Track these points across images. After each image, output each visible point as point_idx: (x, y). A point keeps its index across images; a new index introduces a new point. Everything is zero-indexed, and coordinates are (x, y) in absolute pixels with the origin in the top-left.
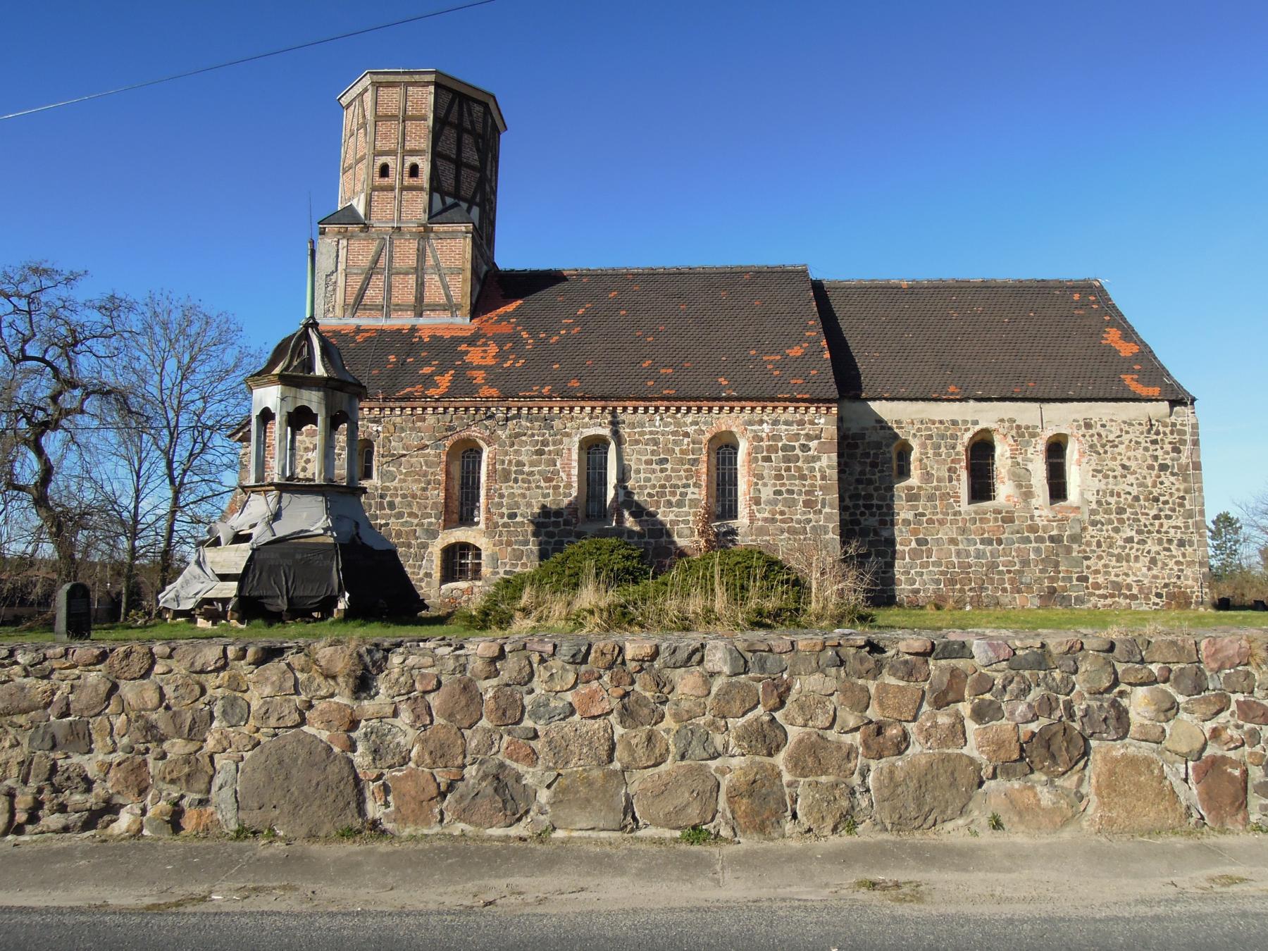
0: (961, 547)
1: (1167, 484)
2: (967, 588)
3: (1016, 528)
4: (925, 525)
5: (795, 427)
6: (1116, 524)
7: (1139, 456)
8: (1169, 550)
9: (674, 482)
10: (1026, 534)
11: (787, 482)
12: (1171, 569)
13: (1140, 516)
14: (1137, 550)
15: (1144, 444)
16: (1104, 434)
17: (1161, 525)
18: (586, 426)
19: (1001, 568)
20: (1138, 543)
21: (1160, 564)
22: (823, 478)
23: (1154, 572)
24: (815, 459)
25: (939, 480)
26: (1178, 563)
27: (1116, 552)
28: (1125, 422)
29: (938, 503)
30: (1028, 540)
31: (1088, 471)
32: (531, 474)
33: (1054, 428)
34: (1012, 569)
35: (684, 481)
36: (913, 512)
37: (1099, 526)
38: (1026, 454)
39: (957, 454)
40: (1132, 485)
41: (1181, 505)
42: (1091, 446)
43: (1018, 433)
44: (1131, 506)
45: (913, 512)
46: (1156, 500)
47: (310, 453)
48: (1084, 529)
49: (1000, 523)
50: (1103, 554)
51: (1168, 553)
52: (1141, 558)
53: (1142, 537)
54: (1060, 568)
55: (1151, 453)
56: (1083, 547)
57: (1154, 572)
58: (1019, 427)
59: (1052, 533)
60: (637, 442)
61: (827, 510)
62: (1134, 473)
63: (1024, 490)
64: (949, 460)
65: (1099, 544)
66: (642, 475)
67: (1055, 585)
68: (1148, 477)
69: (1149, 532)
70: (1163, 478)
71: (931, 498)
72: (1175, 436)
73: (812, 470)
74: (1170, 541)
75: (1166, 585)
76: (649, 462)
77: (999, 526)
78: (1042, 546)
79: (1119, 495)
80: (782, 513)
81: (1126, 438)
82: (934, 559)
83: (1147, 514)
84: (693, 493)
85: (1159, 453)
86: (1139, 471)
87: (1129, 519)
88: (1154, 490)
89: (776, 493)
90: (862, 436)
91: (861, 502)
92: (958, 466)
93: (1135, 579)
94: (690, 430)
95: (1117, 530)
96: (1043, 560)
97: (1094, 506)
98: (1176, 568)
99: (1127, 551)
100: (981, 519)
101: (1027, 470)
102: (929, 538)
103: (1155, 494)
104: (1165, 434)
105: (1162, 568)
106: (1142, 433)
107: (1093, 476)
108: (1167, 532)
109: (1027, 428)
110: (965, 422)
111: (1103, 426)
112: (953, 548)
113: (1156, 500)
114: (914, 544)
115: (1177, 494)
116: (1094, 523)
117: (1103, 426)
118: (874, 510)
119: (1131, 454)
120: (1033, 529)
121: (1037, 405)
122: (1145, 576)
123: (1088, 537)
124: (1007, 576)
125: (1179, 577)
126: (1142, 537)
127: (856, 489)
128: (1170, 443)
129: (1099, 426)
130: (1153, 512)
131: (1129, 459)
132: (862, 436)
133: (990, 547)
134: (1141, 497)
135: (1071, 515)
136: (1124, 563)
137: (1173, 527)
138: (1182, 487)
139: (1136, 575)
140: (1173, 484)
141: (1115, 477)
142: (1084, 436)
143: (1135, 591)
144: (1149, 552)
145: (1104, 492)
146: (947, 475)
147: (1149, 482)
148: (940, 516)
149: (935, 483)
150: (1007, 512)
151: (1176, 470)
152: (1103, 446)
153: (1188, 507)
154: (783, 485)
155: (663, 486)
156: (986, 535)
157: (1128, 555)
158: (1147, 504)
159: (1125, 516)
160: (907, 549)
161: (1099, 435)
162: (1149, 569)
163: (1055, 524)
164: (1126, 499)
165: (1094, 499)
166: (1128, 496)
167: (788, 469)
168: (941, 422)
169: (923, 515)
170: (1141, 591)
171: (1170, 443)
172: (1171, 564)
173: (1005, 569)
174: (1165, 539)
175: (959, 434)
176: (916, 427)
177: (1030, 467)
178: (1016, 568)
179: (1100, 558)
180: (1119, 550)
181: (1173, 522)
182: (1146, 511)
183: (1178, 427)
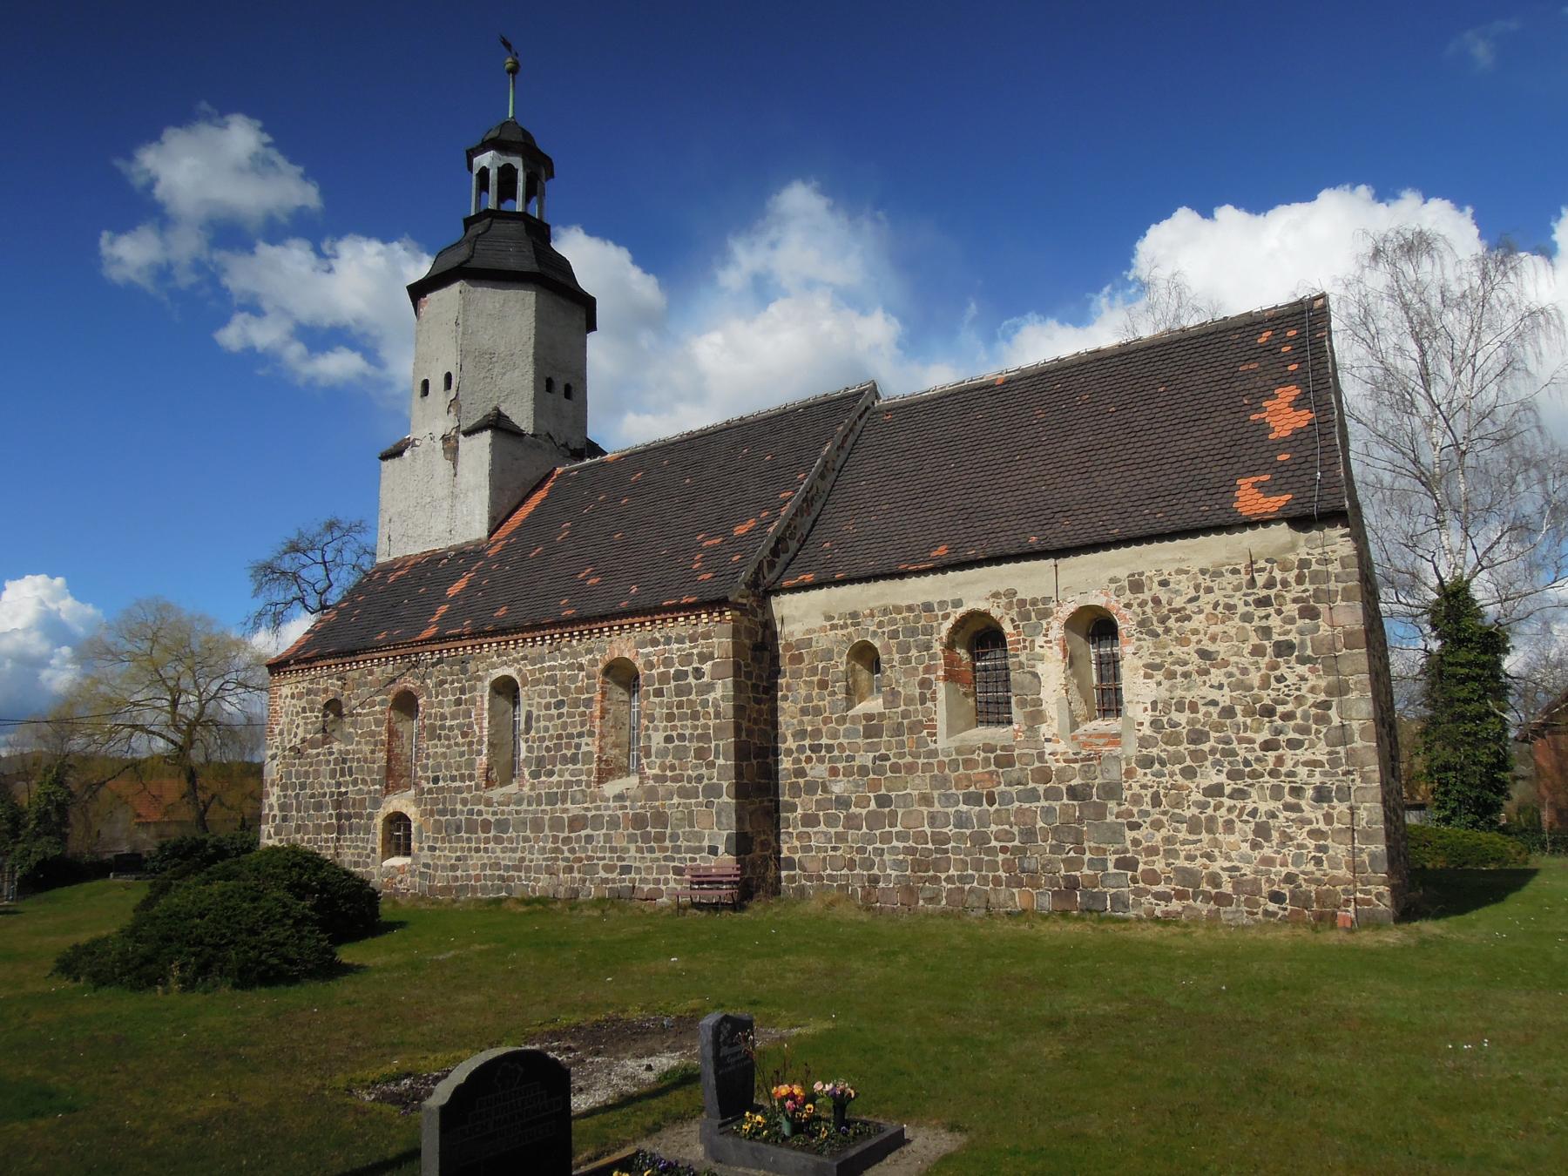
0: (937, 807)
1: (1292, 679)
2: (943, 876)
3: (1015, 775)
4: (889, 774)
5: (688, 645)
6: (1188, 762)
7: (1233, 632)
8: (1295, 808)
9: (570, 730)
10: (1031, 785)
11: (679, 724)
12: (1300, 846)
13: (1235, 745)
14: (1230, 810)
15: (1241, 609)
16: (1164, 598)
17: (1280, 761)
18: (494, 666)
19: (994, 843)
20: (1231, 797)
21: (1275, 835)
22: (717, 715)
23: (1267, 851)
24: (710, 687)
25: (909, 700)
26: (1315, 834)
27: (1187, 814)
28: (1203, 572)
29: (905, 738)
30: (1032, 796)
31: (1137, 669)
32: (451, 728)
33: (1078, 598)
34: (1010, 845)
35: (579, 729)
36: (871, 755)
37: (1157, 766)
38: (1032, 649)
39: (933, 657)
40: (1221, 687)
42: (1142, 624)
43: (1019, 613)
44: (1218, 727)
45: (871, 755)
46: (1269, 712)
48: (1130, 773)
49: (993, 768)
50: (1164, 818)
51: (1293, 815)
52: (1238, 825)
53: (1240, 785)
54: (1086, 845)
55: (1256, 623)
56: (1127, 806)
57: (1267, 851)
58: (1022, 603)
59: (1073, 783)
60: (537, 682)
61: (721, 761)
62: (1226, 663)
63: (1029, 709)
64: (921, 668)
65: (1155, 800)
66: (542, 724)
67: (1078, 874)
68: (1252, 668)
69: (1255, 775)
70: (1283, 670)
71: (898, 730)
72: (1307, 585)
73: (705, 704)
74: (1297, 791)
75: (1290, 878)
76: (548, 707)
77: (991, 773)
78: (1057, 805)
79: (1194, 708)
80: (672, 768)
81: (1206, 600)
82: (899, 828)
83: (1251, 741)
84: (587, 744)
85: (1275, 622)
86: (1234, 659)
87: (1213, 751)
88: (1263, 693)
89: (668, 739)
90: (808, 644)
91: (807, 742)
92: (933, 677)
93: (1227, 864)
94: (584, 660)
95: (1189, 773)
96: (1056, 830)
97: (1147, 730)
98: (1311, 843)
99: (1210, 811)
100: (966, 762)
101: (1035, 675)
102: (893, 794)
103: (1267, 701)
104: (1285, 583)
105: (1283, 844)
106: (1237, 588)
107: (1147, 676)
108: (1291, 774)
109: (1034, 602)
110: (942, 604)
111: (1164, 583)
112: (925, 810)
113: (1269, 712)
114: (873, 805)
115: (1311, 698)
116: (1146, 762)
117: (1164, 583)
118: (823, 753)
119: (1213, 629)
120: (1044, 775)
121: (1052, 561)
122: (1246, 859)
123: (1136, 788)
124: (1001, 857)
125: (1318, 862)
126: (1240, 785)
127: (801, 722)
128: (1295, 601)
129: (1155, 585)
130: (1265, 735)
131: (1213, 639)
132: (808, 644)
133: (977, 808)
134: (1238, 709)
135: (1105, 750)
137: (1306, 764)
138: (1323, 683)
139: (1228, 858)
140: (1303, 679)
141: (1186, 675)
142: (1128, 606)
143: (1227, 888)
144: (1254, 813)
145: (1167, 704)
146: (917, 691)
147: (1255, 678)
148: (909, 759)
149: (903, 707)
150: (1003, 748)
151: (1309, 652)
152: (1163, 620)
153: (1336, 721)
154: (674, 728)
155: (560, 737)
156: (972, 789)
157: (1212, 819)
158: (1249, 721)
159: (1206, 747)
160: (864, 812)
161: (1157, 601)
162: (1255, 846)
163: (1077, 766)
164: (1208, 714)
165: (1146, 718)
166: (1211, 709)
167: (680, 706)
168: (910, 608)
169: (885, 758)
170: (1238, 884)
171: (1295, 601)
172: (1302, 836)
173: (998, 845)
174: (1287, 787)
175: (935, 624)
176: (876, 620)
177: (1040, 668)
178: (1016, 843)
179: (1157, 825)
180: (1195, 811)
181: (1304, 754)
182: (1249, 734)
183: (1314, 567)
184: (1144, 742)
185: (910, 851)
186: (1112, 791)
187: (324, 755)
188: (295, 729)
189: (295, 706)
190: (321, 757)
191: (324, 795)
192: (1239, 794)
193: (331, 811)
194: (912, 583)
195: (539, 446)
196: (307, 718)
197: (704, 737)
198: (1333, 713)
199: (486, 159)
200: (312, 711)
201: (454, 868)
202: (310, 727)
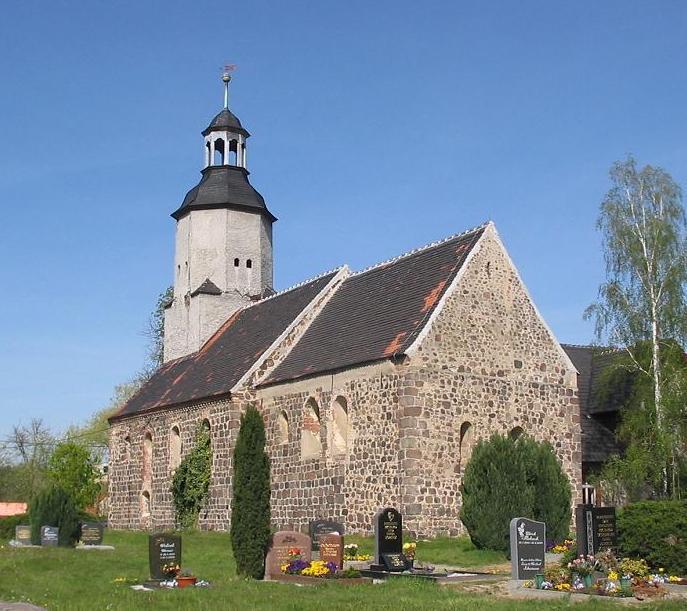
30: (322, 483)
41: (397, 448)
46: (384, 445)
113: (384, 445)
119: (372, 407)
136: (365, 500)
162: (378, 504)
180: (363, 488)
181: (392, 464)
184: (352, 458)
185: (293, 508)
186: (342, 480)
192: (375, 481)
194: (299, 384)
195: (230, 297)
197: (225, 456)
198: (400, 445)
199: (214, 136)
201: (161, 517)
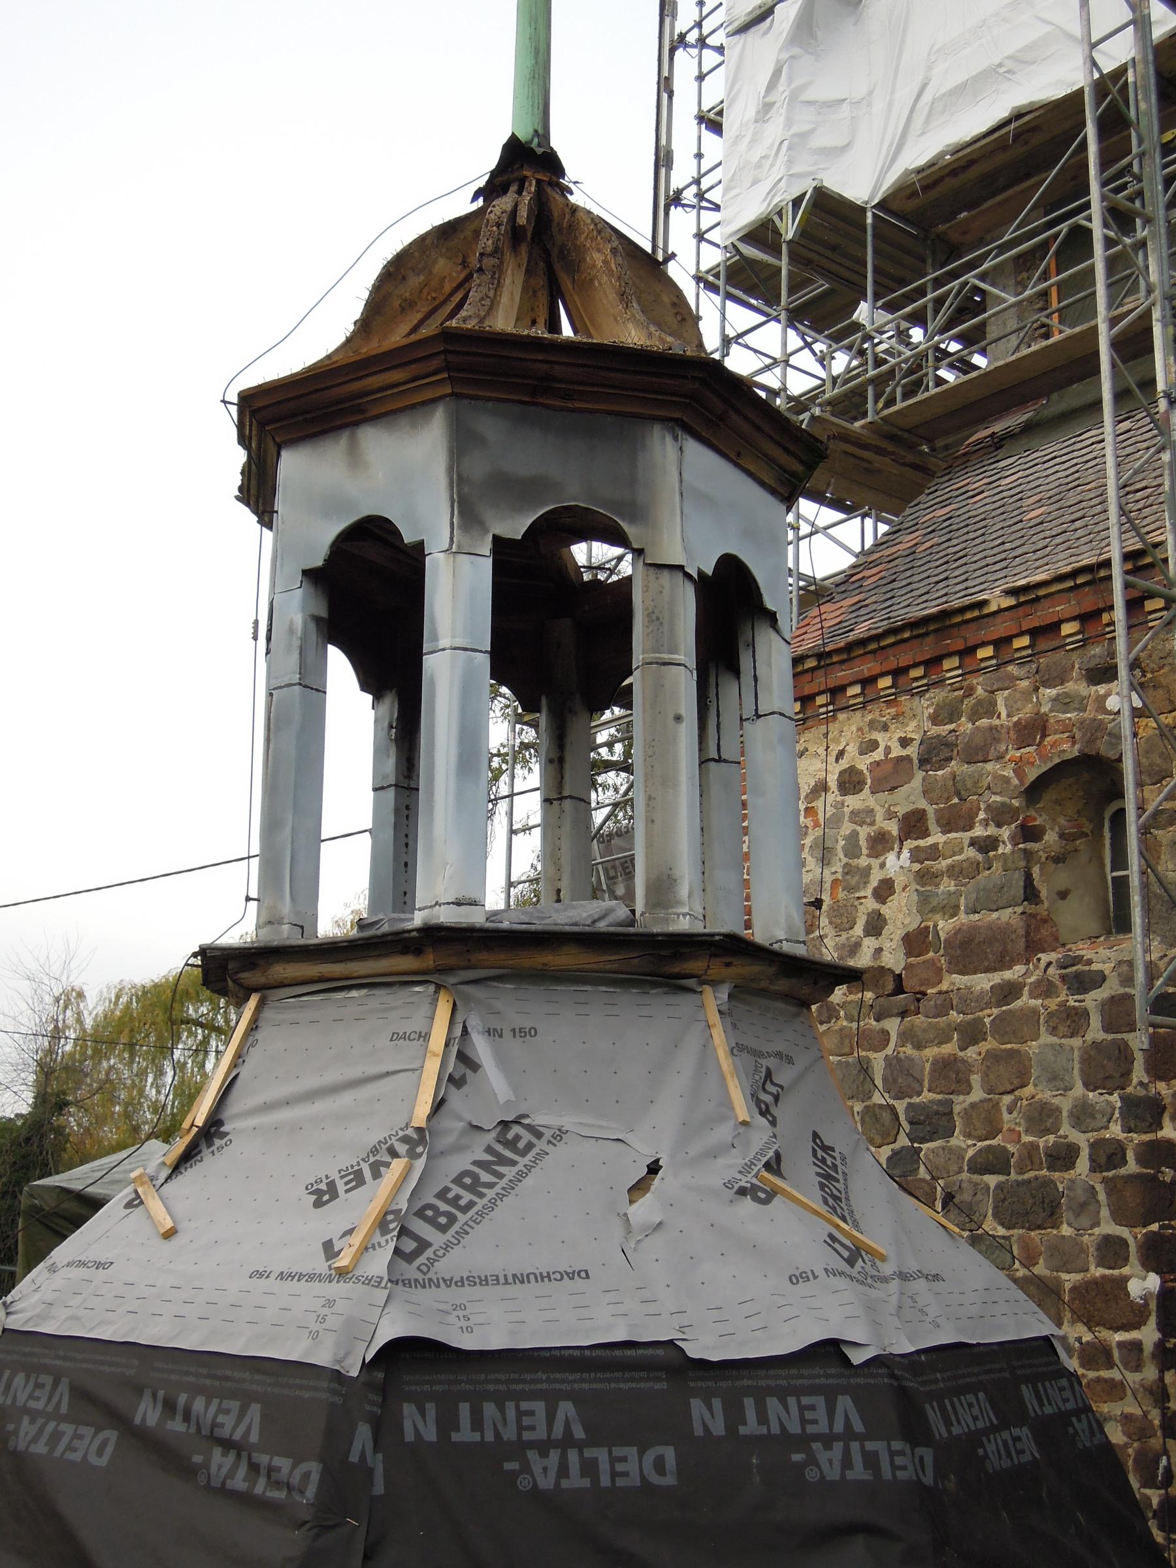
47: (891, 859)
187: (1045, 989)
188: (871, 904)
189: (862, 817)
190: (1025, 1001)
191: (1064, 1157)
193: (1110, 1228)
196: (934, 852)
200: (953, 821)
202: (948, 885)
